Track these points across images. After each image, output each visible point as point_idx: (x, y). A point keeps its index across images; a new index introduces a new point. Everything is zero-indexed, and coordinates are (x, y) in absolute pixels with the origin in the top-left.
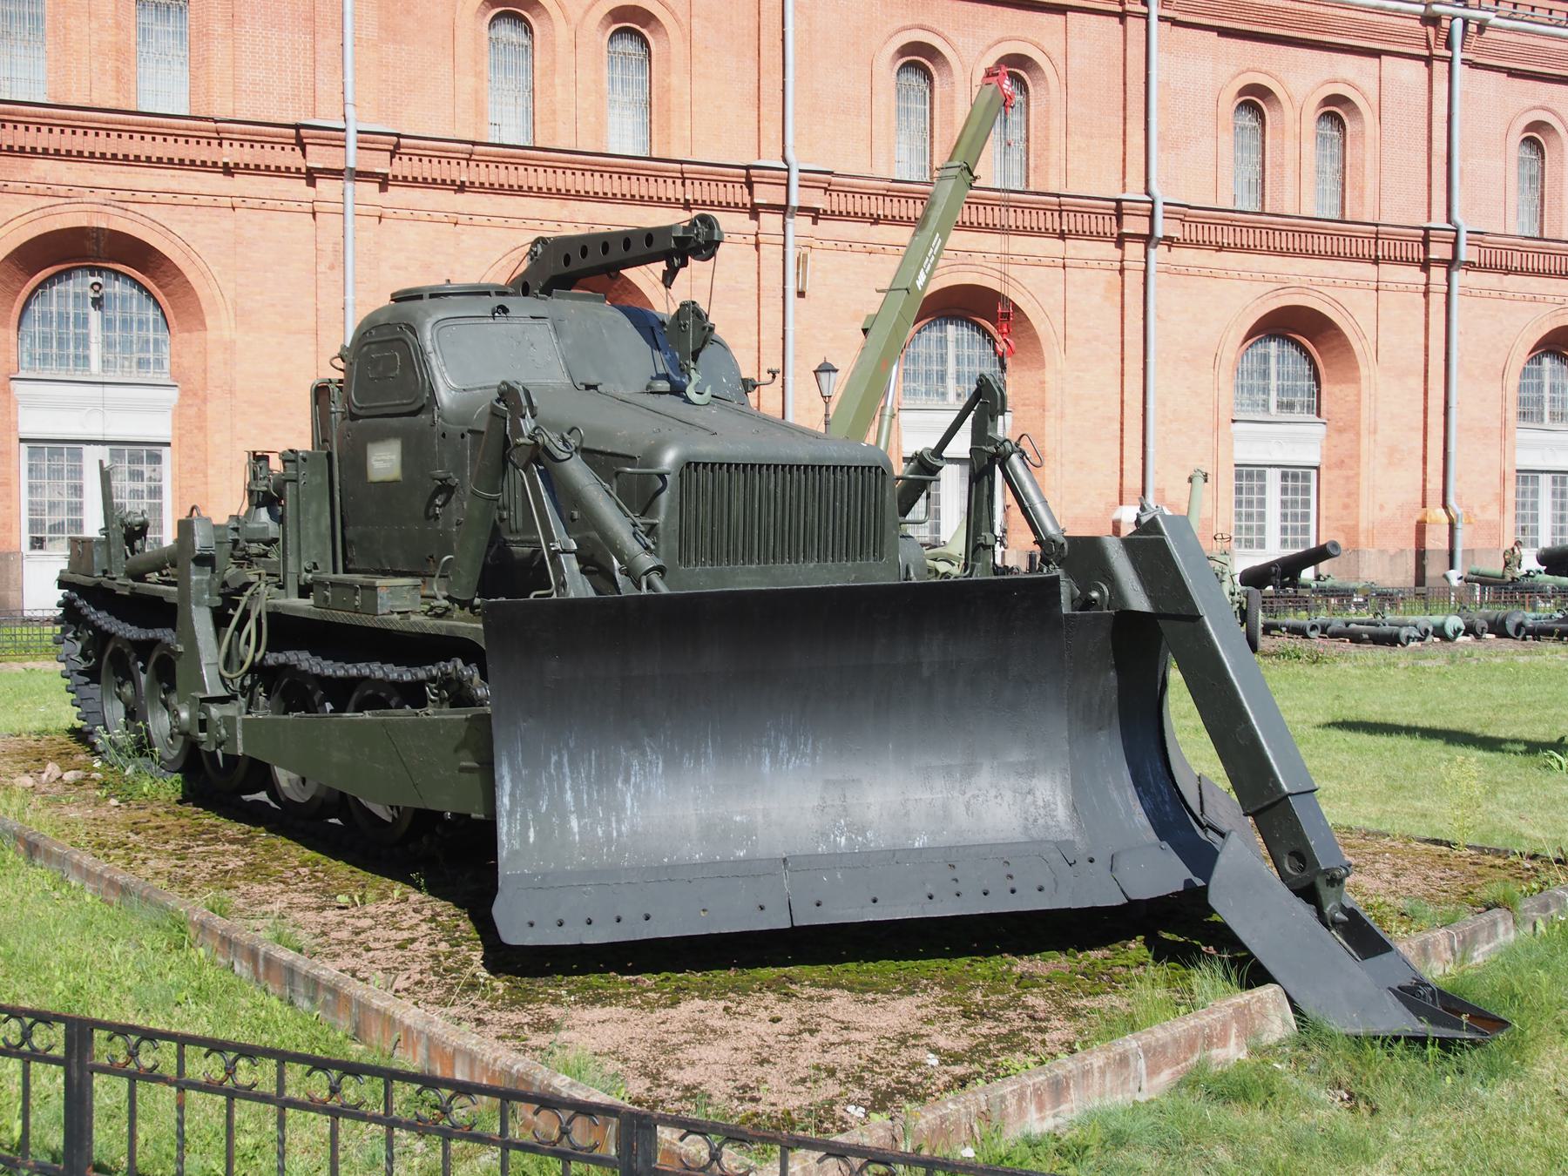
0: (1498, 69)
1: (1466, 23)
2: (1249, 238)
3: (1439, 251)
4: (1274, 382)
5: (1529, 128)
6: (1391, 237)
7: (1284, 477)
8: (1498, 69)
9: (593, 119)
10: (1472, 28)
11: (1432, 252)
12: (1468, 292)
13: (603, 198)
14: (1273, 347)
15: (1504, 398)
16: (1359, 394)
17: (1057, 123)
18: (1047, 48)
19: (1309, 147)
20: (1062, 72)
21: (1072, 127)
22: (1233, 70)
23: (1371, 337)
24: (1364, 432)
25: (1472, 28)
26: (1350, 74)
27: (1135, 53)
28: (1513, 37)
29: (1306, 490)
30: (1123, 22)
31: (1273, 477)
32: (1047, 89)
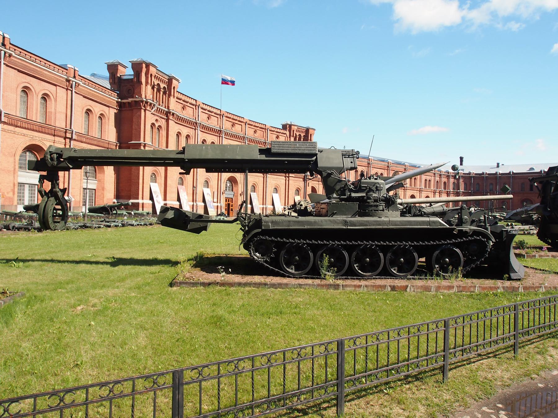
1: (5, 53)
10: (7, 55)
15: (15, 162)
25: (7, 55)
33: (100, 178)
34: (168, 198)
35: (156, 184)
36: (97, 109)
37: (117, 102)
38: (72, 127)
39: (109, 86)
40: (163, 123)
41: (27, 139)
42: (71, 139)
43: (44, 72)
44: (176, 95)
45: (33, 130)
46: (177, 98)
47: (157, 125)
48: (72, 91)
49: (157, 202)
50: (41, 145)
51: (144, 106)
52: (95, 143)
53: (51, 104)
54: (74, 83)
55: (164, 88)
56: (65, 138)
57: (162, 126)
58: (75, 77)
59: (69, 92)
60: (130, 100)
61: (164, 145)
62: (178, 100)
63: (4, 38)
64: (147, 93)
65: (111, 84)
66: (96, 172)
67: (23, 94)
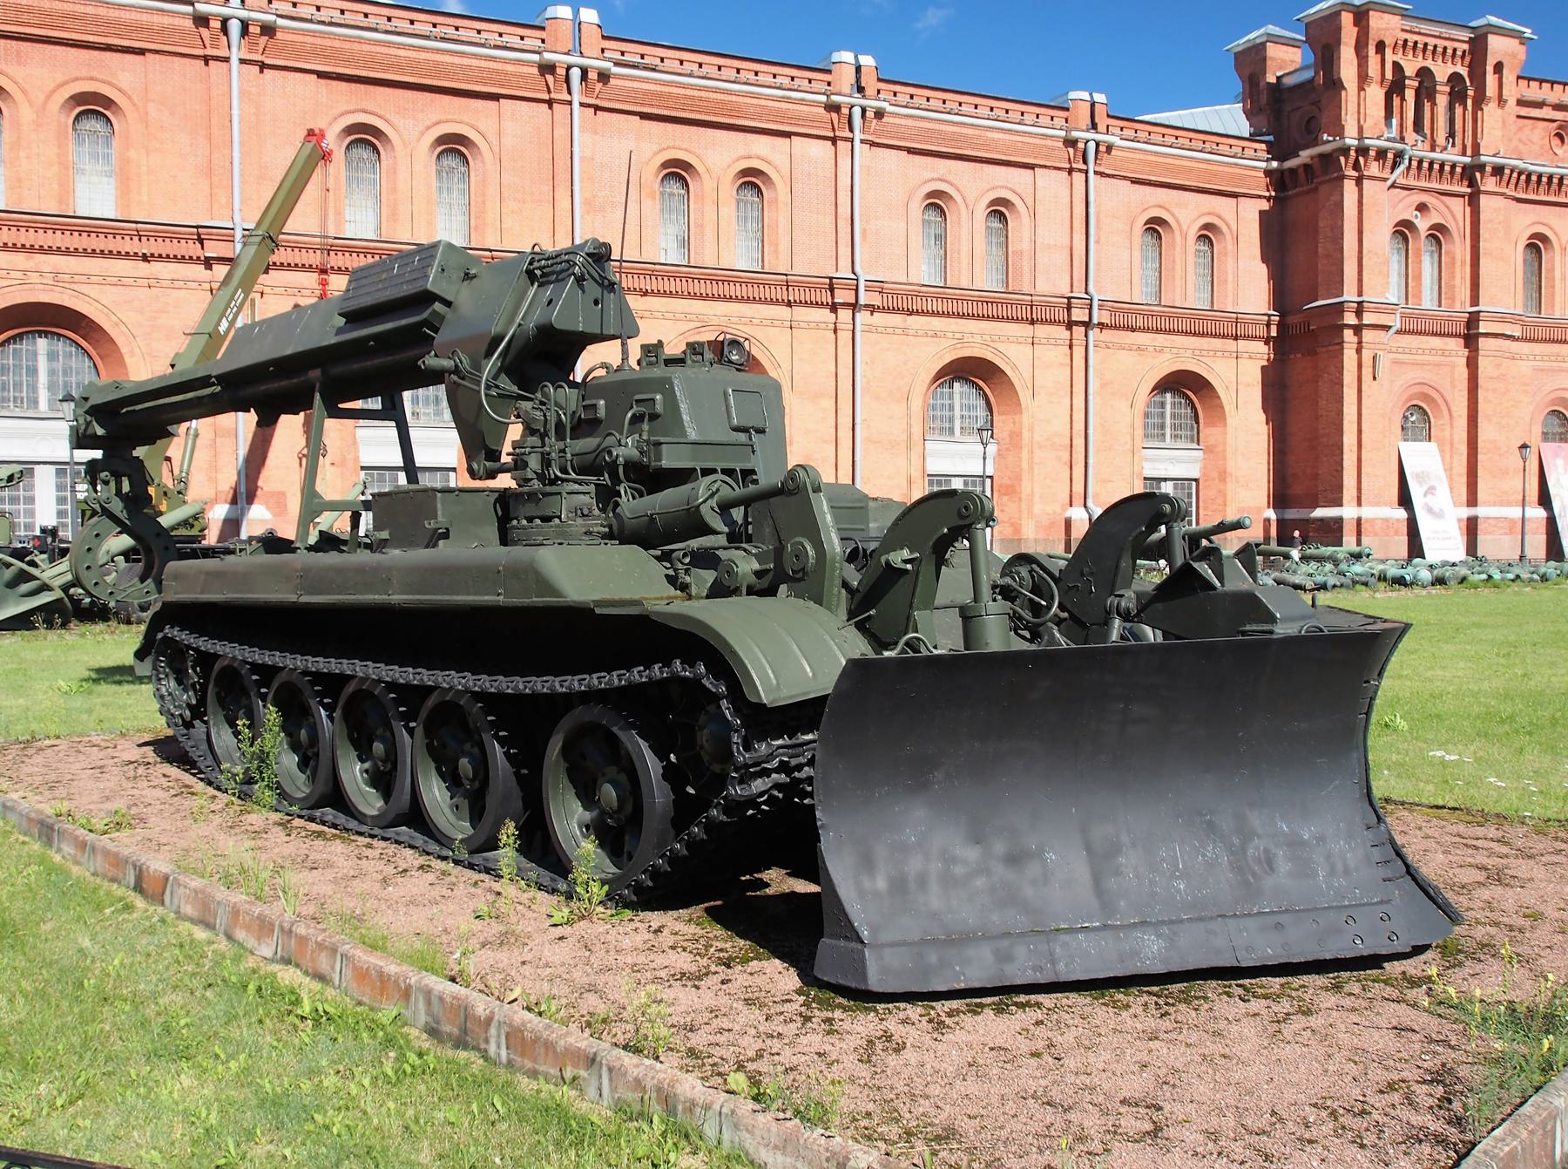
2: (671, 286)
3: (842, 296)
5: (931, 195)
6: (799, 285)
9: (56, 186)
11: (833, 296)
12: (870, 329)
13: (67, 252)
15: (909, 416)
17: (492, 191)
18: (482, 128)
19: (729, 211)
20: (496, 149)
21: (505, 194)
22: (655, 148)
25: (870, 114)
26: (763, 151)
27: (561, 132)
28: (910, 122)
30: (551, 107)
33: (1212, 441)
34: (1481, 496)
35: (1432, 447)
36: (1187, 212)
37: (1268, 173)
38: (1091, 289)
39: (1244, 128)
40: (1454, 213)
41: (945, 343)
42: (1087, 325)
43: (990, 134)
44: (1512, 91)
45: (963, 316)
46: (1520, 103)
47: (1423, 224)
48: (1086, 172)
49: (1430, 511)
50: (989, 357)
51: (1356, 166)
52: (1183, 326)
53: (1019, 226)
54: (1092, 145)
55: (1455, 78)
56: (1070, 325)
57: (1451, 225)
58: (1094, 126)
59: (1078, 178)
60: (1305, 155)
61: (1464, 293)
62: (1524, 111)
63: (858, 69)
64: (1362, 113)
65: (1248, 114)
66: (1197, 422)
67: (933, 216)
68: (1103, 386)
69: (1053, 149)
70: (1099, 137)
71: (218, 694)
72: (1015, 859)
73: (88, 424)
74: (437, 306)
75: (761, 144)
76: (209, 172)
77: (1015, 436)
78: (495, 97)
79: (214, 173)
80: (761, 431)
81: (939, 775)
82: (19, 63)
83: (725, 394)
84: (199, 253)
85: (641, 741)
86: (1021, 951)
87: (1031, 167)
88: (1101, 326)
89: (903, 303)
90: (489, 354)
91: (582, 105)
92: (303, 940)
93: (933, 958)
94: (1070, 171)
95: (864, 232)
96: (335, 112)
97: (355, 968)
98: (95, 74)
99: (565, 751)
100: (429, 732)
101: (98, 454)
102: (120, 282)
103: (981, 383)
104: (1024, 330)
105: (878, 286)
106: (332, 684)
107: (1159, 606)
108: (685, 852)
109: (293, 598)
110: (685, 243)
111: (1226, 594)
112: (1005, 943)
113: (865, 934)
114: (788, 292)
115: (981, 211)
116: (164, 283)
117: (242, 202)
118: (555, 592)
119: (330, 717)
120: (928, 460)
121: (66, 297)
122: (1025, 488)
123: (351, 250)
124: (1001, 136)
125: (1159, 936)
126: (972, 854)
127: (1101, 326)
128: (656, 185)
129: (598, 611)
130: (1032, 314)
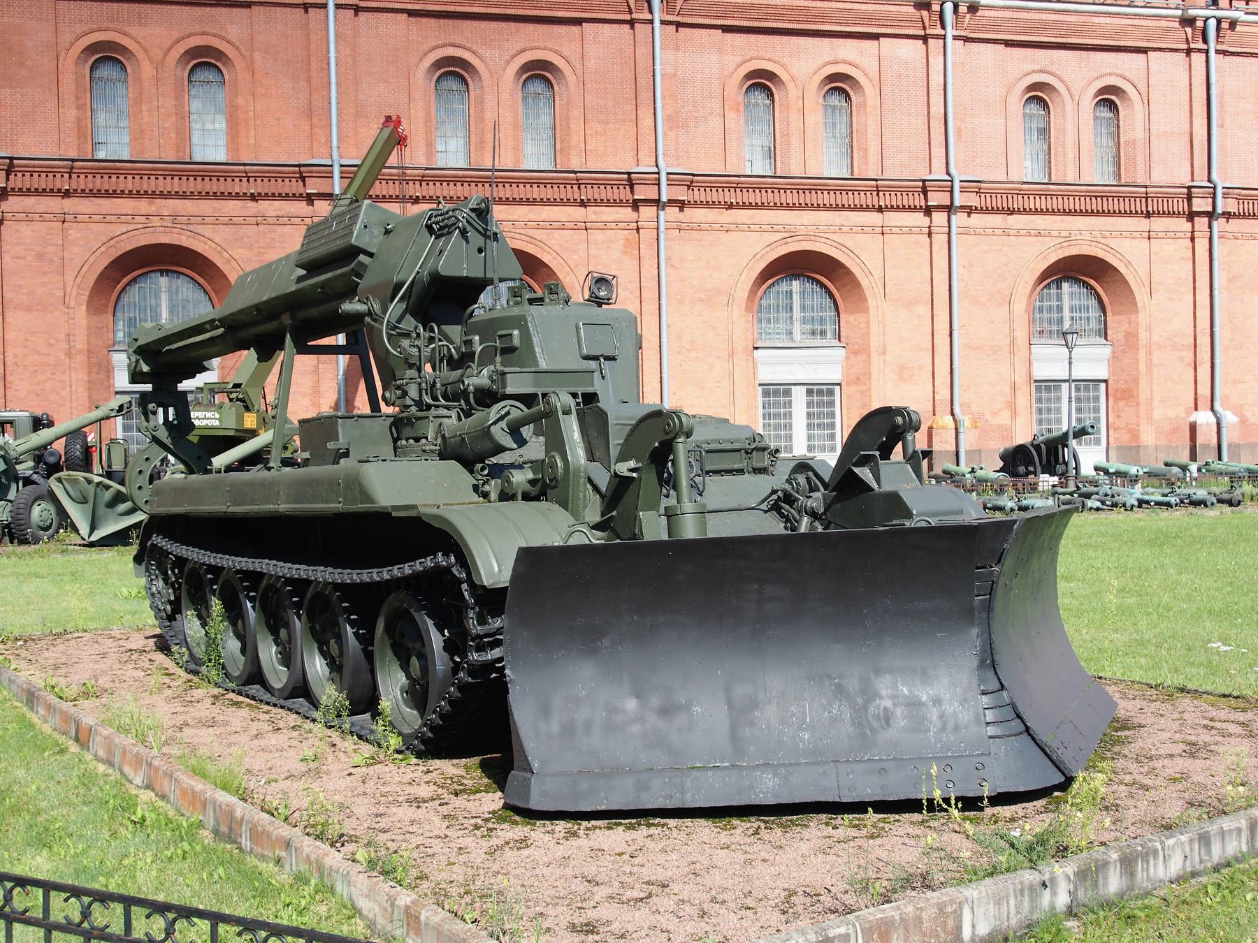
0: (995, 41)
2: (756, 197)
3: (935, 199)
4: (797, 313)
6: (890, 190)
7: (809, 392)
8: (995, 41)
9: (174, 136)
11: (927, 198)
12: (967, 231)
13: (184, 196)
14: (796, 285)
15: (1012, 320)
16: (868, 323)
17: (577, 113)
18: (565, 53)
19: (816, 118)
20: (579, 72)
21: (589, 116)
22: (738, 59)
23: (877, 274)
24: (874, 354)
26: (848, 56)
27: (643, 51)
29: (832, 404)
30: (632, 28)
31: (799, 395)
32: (567, 86)
38: (1214, 176)
41: (1050, 242)
42: (1211, 215)
43: (1096, 20)
45: (1069, 213)
48: (1207, 52)
53: (1132, 115)
54: (1212, 23)
56: (1191, 216)
59: (1198, 58)
67: (1035, 109)
68: (1231, 280)
69: (1168, 30)
70: (1219, 13)
71: (188, 591)
72: (666, 711)
73: (137, 361)
74: (362, 258)
75: (848, 49)
76: (309, 114)
77: (1131, 338)
78: (578, 22)
79: (314, 113)
80: (608, 358)
81: (606, 642)
82: (140, 24)
83: (577, 328)
84: (301, 190)
85: (428, 620)
86: (657, 784)
87: (1143, 51)
88: (1228, 215)
89: (1003, 201)
90: (392, 301)
91: (663, 22)
92: (157, 769)
93: (584, 786)
94: (1188, 52)
95: (958, 131)
96: (425, 47)
97: (182, 789)
98: (208, 29)
99: (388, 629)
100: (311, 619)
101: (148, 387)
102: (231, 221)
103: (1092, 282)
104: (1142, 224)
105: (975, 186)
106: (254, 578)
107: (838, 506)
108: (448, 708)
109: (223, 508)
110: (771, 154)
111: (880, 494)
112: (645, 776)
113: (535, 765)
114: (877, 196)
115: (1088, 102)
116: (271, 220)
117: (339, 140)
118: (370, 500)
119: (253, 607)
120: (1035, 365)
121: (184, 238)
122: (1143, 392)
123: (442, 180)
124: (1109, 20)
125: (775, 775)
126: (631, 704)
127: (1228, 215)
128: (741, 98)
129: (394, 514)
130: (1146, 206)
